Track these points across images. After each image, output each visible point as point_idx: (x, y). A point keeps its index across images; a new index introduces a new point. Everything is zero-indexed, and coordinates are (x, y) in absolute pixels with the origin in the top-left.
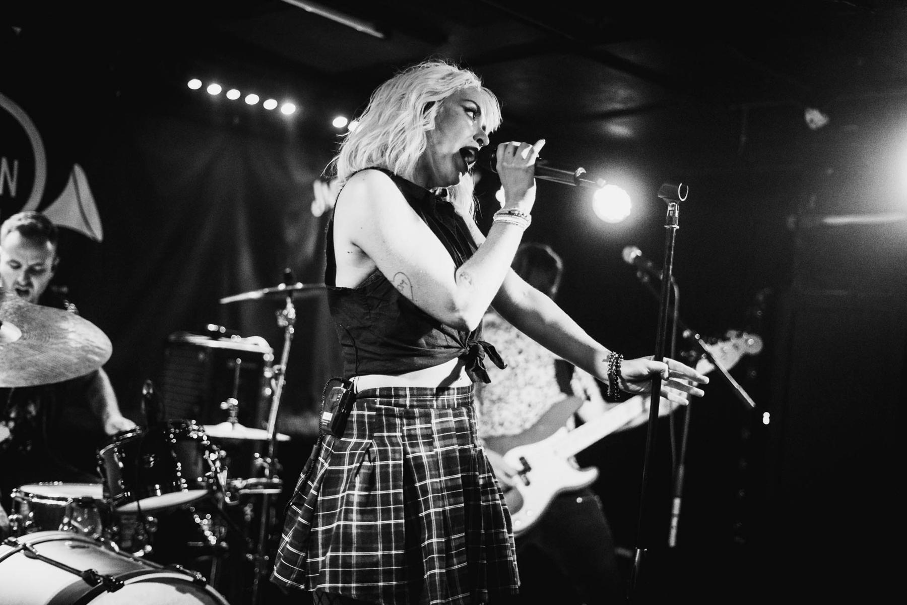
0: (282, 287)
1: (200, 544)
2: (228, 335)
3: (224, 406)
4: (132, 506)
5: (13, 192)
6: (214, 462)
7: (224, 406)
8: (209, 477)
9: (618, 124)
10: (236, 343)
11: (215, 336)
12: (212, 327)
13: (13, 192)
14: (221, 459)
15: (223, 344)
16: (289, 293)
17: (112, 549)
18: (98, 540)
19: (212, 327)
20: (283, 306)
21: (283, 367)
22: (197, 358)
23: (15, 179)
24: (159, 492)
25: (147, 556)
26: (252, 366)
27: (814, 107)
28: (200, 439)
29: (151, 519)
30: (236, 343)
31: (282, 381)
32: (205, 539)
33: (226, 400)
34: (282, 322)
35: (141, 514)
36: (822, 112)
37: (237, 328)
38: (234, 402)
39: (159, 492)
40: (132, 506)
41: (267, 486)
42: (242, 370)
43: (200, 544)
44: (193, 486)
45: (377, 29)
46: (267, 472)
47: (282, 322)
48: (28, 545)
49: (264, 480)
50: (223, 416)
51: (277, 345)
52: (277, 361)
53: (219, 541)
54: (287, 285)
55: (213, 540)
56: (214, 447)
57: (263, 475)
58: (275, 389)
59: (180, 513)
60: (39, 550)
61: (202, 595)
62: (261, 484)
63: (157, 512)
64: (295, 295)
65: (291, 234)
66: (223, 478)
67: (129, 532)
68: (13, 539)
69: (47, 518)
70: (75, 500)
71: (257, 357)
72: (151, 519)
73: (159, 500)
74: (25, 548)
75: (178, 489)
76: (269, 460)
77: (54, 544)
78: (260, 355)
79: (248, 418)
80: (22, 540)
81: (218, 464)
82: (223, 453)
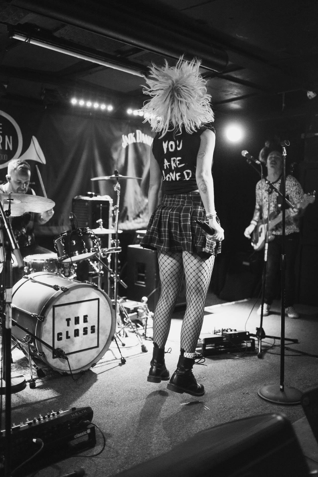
3: (97, 222)
5: (11, 149)
8: (95, 248)
13: (11, 149)
17: (63, 277)
18: (56, 274)
21: (118, 206)
22: (85, 205)
23: (11, 143)
25: (74, 278)
26: (106, 206)
27: (310, 91)
31: (118, 211)
34: (115, 189)
36: (313, 92)
41: (116, 250)
42: (102, 207)
46: (115, 244)
47: (115, 189)
48: (32, 278)
49: (114, 248)
50: (97, 226)
52: (115, 203)
57: (114, 246)
60: (36, 279)
61: (96, 291)
62: (114, 249)
63: (77, 262)
65: (115, 156)
68: (26, 276)
69: (37, 268)
70: (47, 260)
71: (107, 203)
74: (31, 279)
75: (85, 252)
76: (116, 240)
77: (43, 276)
79: (106, 226)
80: (29, 276)
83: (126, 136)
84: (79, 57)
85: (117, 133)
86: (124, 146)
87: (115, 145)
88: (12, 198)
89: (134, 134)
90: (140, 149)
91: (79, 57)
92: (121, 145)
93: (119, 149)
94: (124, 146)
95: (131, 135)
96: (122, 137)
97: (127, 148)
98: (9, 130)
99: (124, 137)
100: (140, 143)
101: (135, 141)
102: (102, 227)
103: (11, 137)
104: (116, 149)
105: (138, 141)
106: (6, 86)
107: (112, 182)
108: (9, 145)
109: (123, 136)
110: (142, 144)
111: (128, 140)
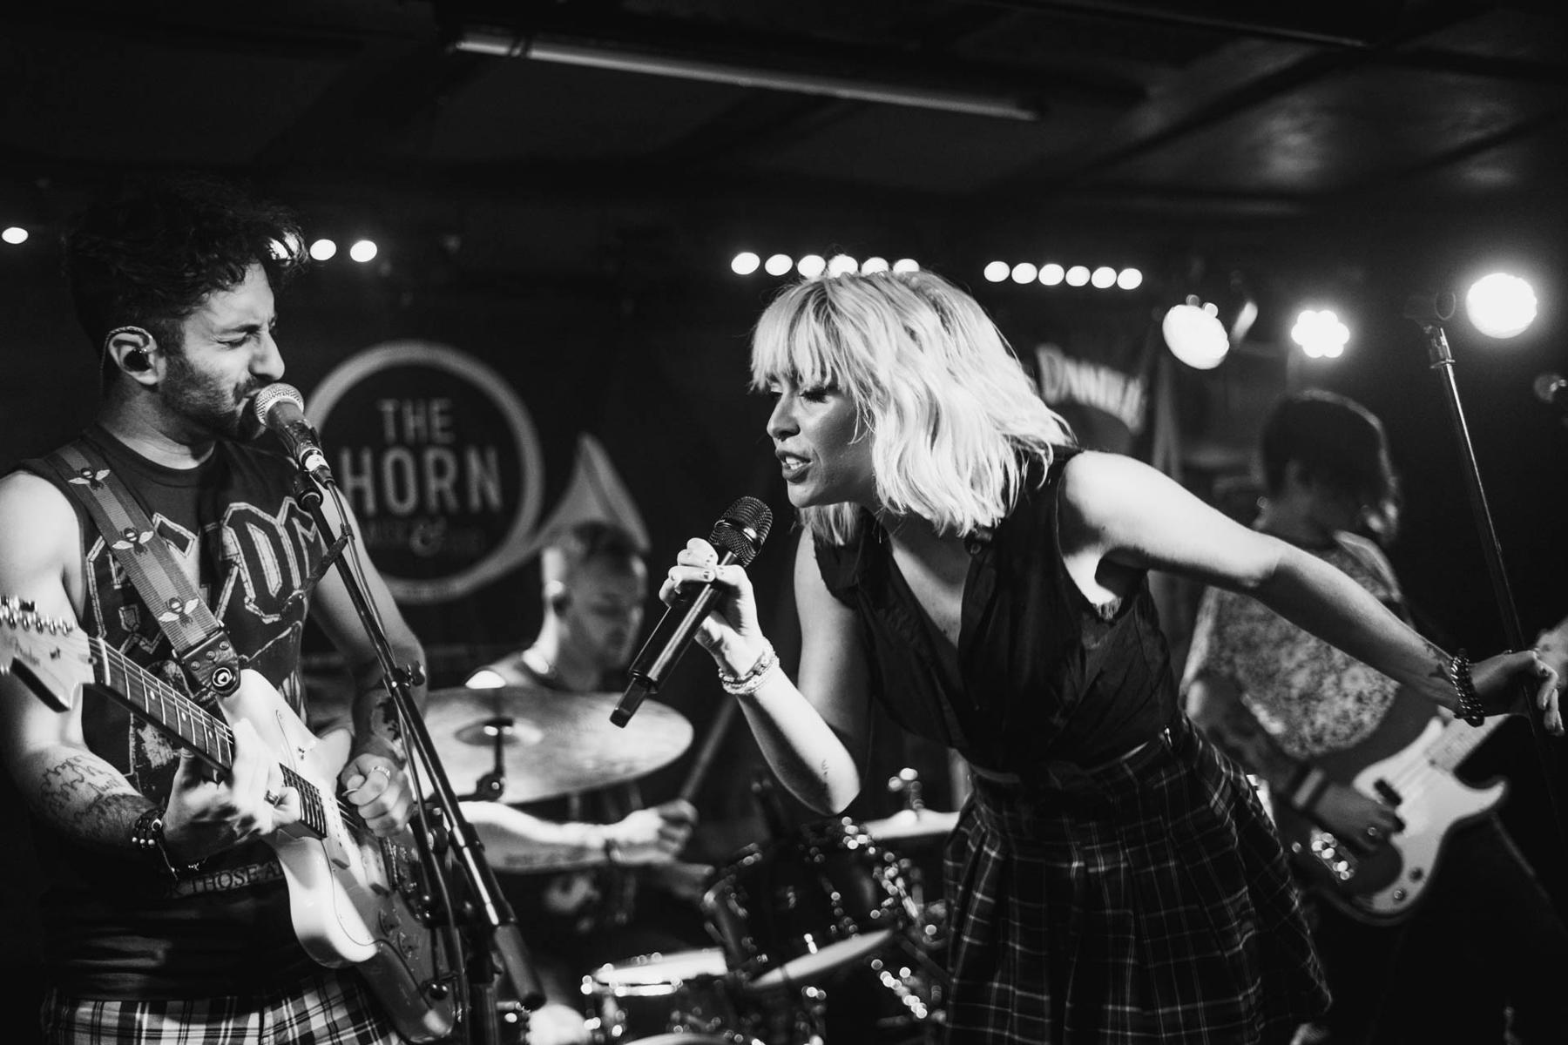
1: (899, 1020)
3: (894, 784)
4: (775, 976)
6: (893, 880)
7: (894, 784)
14: (902, 874)
24: (812, 947)
28: (863, 848)
29: (812, 992)
32: (907, 1011)
33: (896, 773)
35: (793, 988)
38: (908, 774)
39: (812, 947)
40: (775, 976)
43: (899, 1020)
44: (866, 927)
45: (1023, 106)
50: (898, 802)
53: (931, 1008)
55: (919, 1010)
56: (889, 855)
59: (856, 975)
66: (913, 908)
67: (780, 1020)
72: (812, 992)
73: (816, 959)
81: (900, 883)
82: (905, 863)
84: (744, 80)
88: (507, 714)
91: (744, 80)
98: (477, 424)
103: (492, 457)
106: (453, 243)
108: (485, 483)
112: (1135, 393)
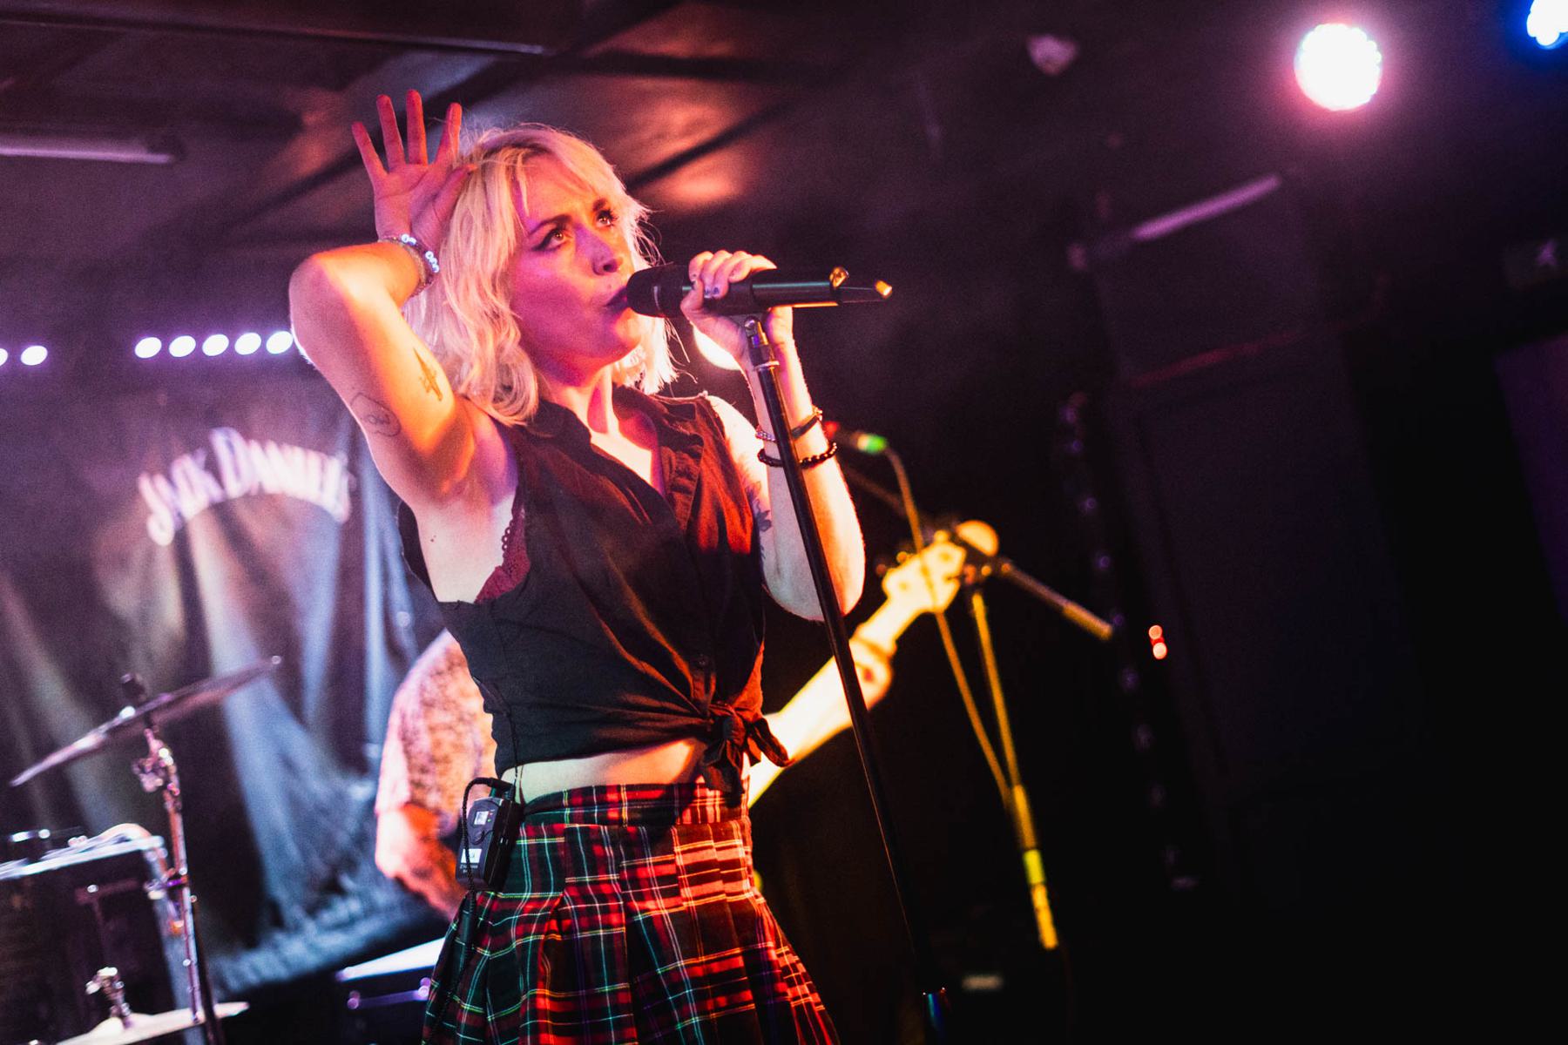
0: (128, 712)
2: (60, 843)
3: (92, 988)
9: (693, 177)
10: (80, 851)
11: (32, 851)
12: (20, 837)
15: (54, 861)
16: (146, 719)
19: (20, 837)
20: (145, 750)
30: (80, 851)
31: (188, 897)
33: (92, 975)
34: (150, 783)
37: (74, 822)
51: (158, 825)
54: (136, 706)
58: (180, 923)
64: (158, 719)
65: (122, 597)
78: (138, 854)
83: (161, 482)
85: (100, 478)
86: (161, 532)
87: (106, 540)
89: (202, 458)
90: (258, 528)
92: (143, 530)
93: (138, 555)
94: (161, 532)
95: (188, 468)
96: (135, 492)
97: (182, 542)
99: (152, 490)
100: (247, 497)
101: (216, 493)
102: (125, 1008)
104: (122, 562)
105: (234, 489)
107: (126, 750)
109: (145, 485)
110: (260, 498)
111: (173, 500)
112: (336, 467)
